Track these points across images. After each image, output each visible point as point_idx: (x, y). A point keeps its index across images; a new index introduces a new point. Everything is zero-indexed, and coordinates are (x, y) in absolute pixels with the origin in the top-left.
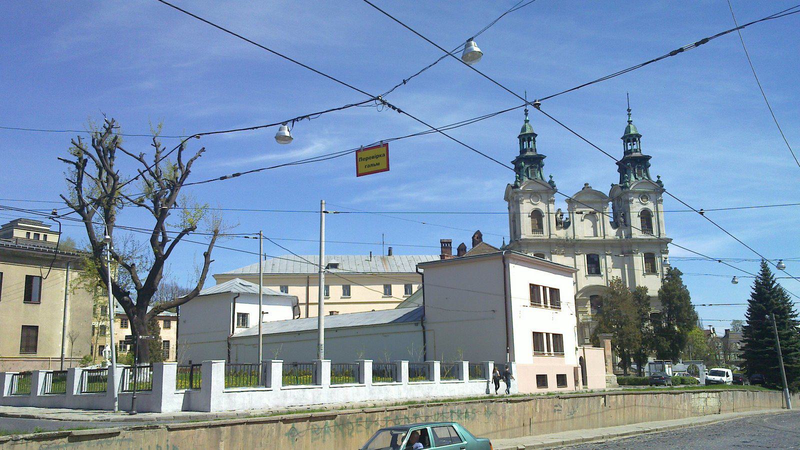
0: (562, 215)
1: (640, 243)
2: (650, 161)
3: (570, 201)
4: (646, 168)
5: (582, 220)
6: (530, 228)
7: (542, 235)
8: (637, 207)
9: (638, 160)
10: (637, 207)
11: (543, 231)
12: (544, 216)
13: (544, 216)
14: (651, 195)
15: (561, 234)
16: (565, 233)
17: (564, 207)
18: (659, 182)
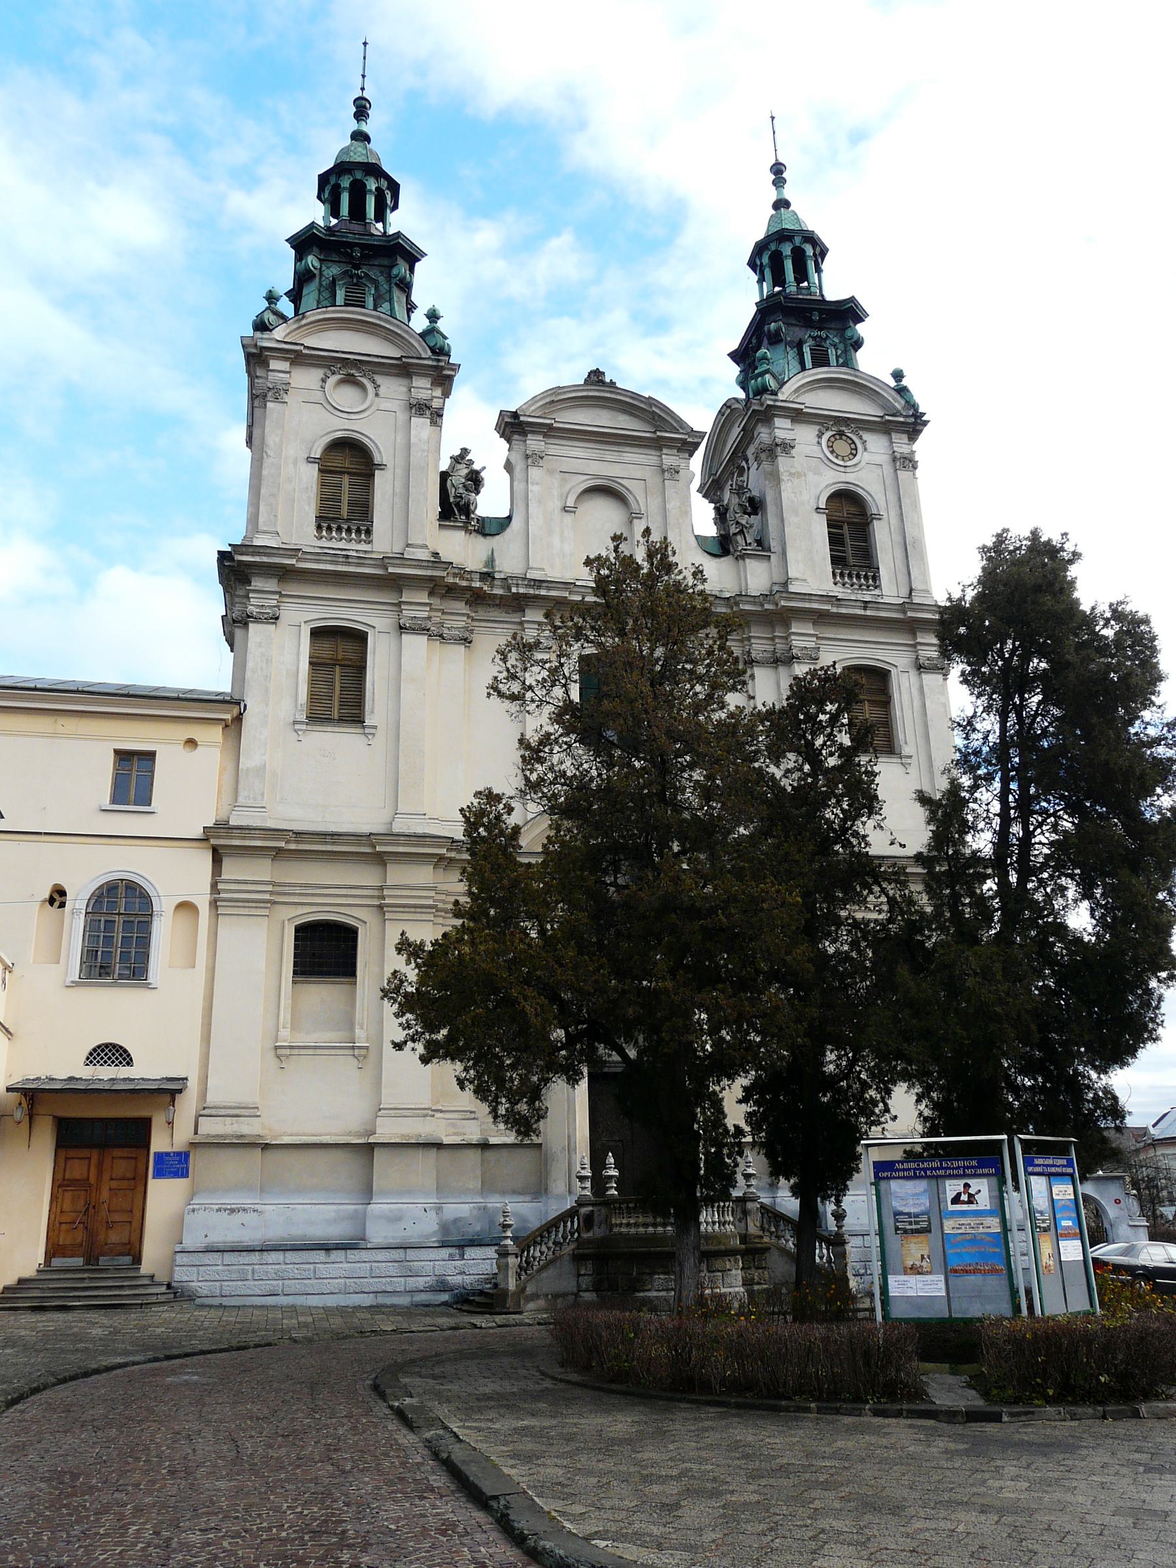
0: (475, 481)
1: (825, 617)
2: (861, 328)
3: (512, 426)
4: (845, 351)
5: (565, 509)
6: (308, 510)
7: (363, 547)
8: (810, 475)
9: (816, 317)
10: (810, 475)
11: (369, 532)
12: (381, 467)
13: (381, 467)
14: (866, 436)
15: (461, 550)
16: (484, 556)
17: (491, 454)
18: (902, 391)
